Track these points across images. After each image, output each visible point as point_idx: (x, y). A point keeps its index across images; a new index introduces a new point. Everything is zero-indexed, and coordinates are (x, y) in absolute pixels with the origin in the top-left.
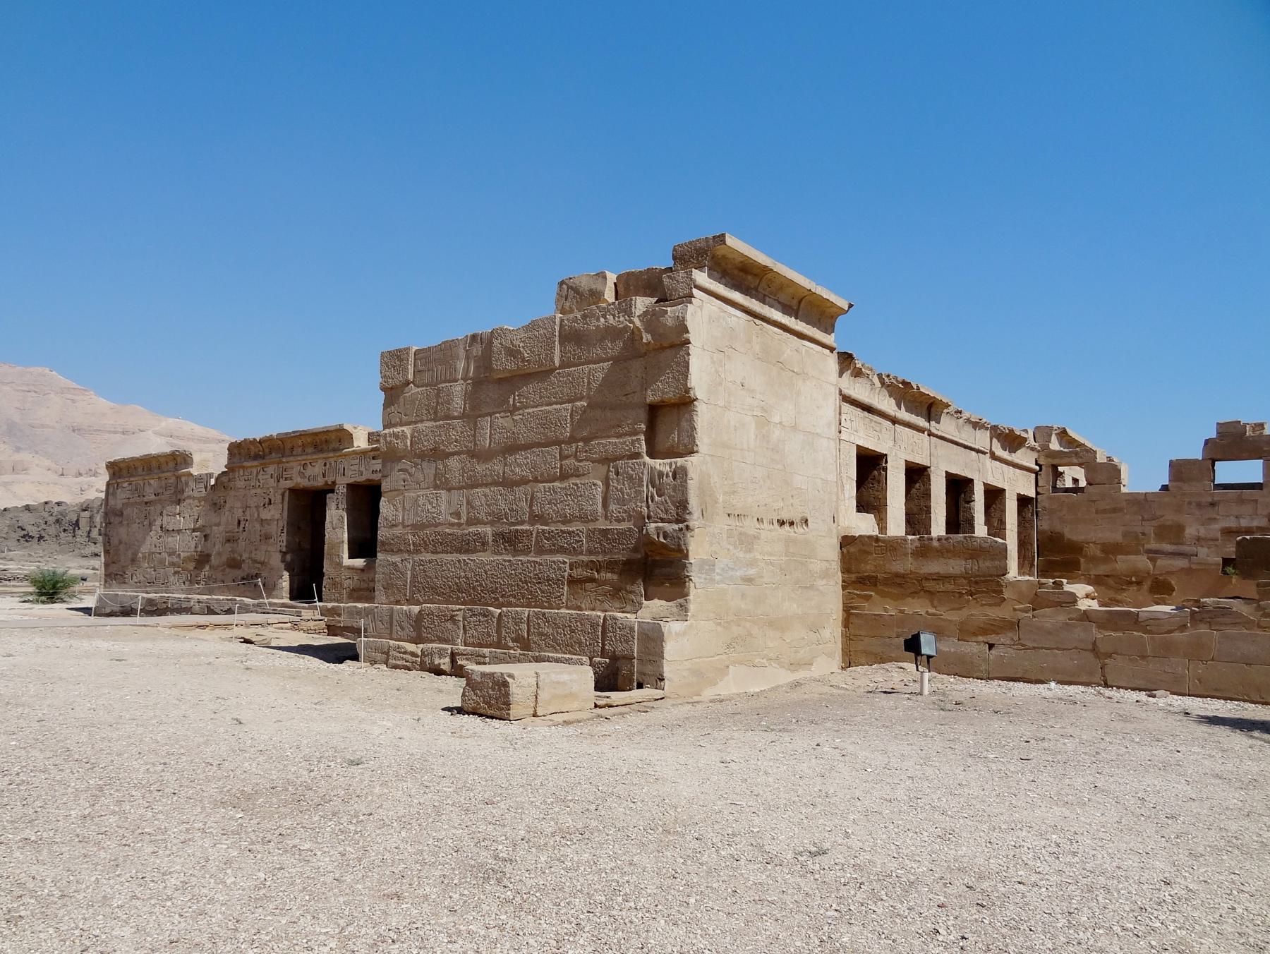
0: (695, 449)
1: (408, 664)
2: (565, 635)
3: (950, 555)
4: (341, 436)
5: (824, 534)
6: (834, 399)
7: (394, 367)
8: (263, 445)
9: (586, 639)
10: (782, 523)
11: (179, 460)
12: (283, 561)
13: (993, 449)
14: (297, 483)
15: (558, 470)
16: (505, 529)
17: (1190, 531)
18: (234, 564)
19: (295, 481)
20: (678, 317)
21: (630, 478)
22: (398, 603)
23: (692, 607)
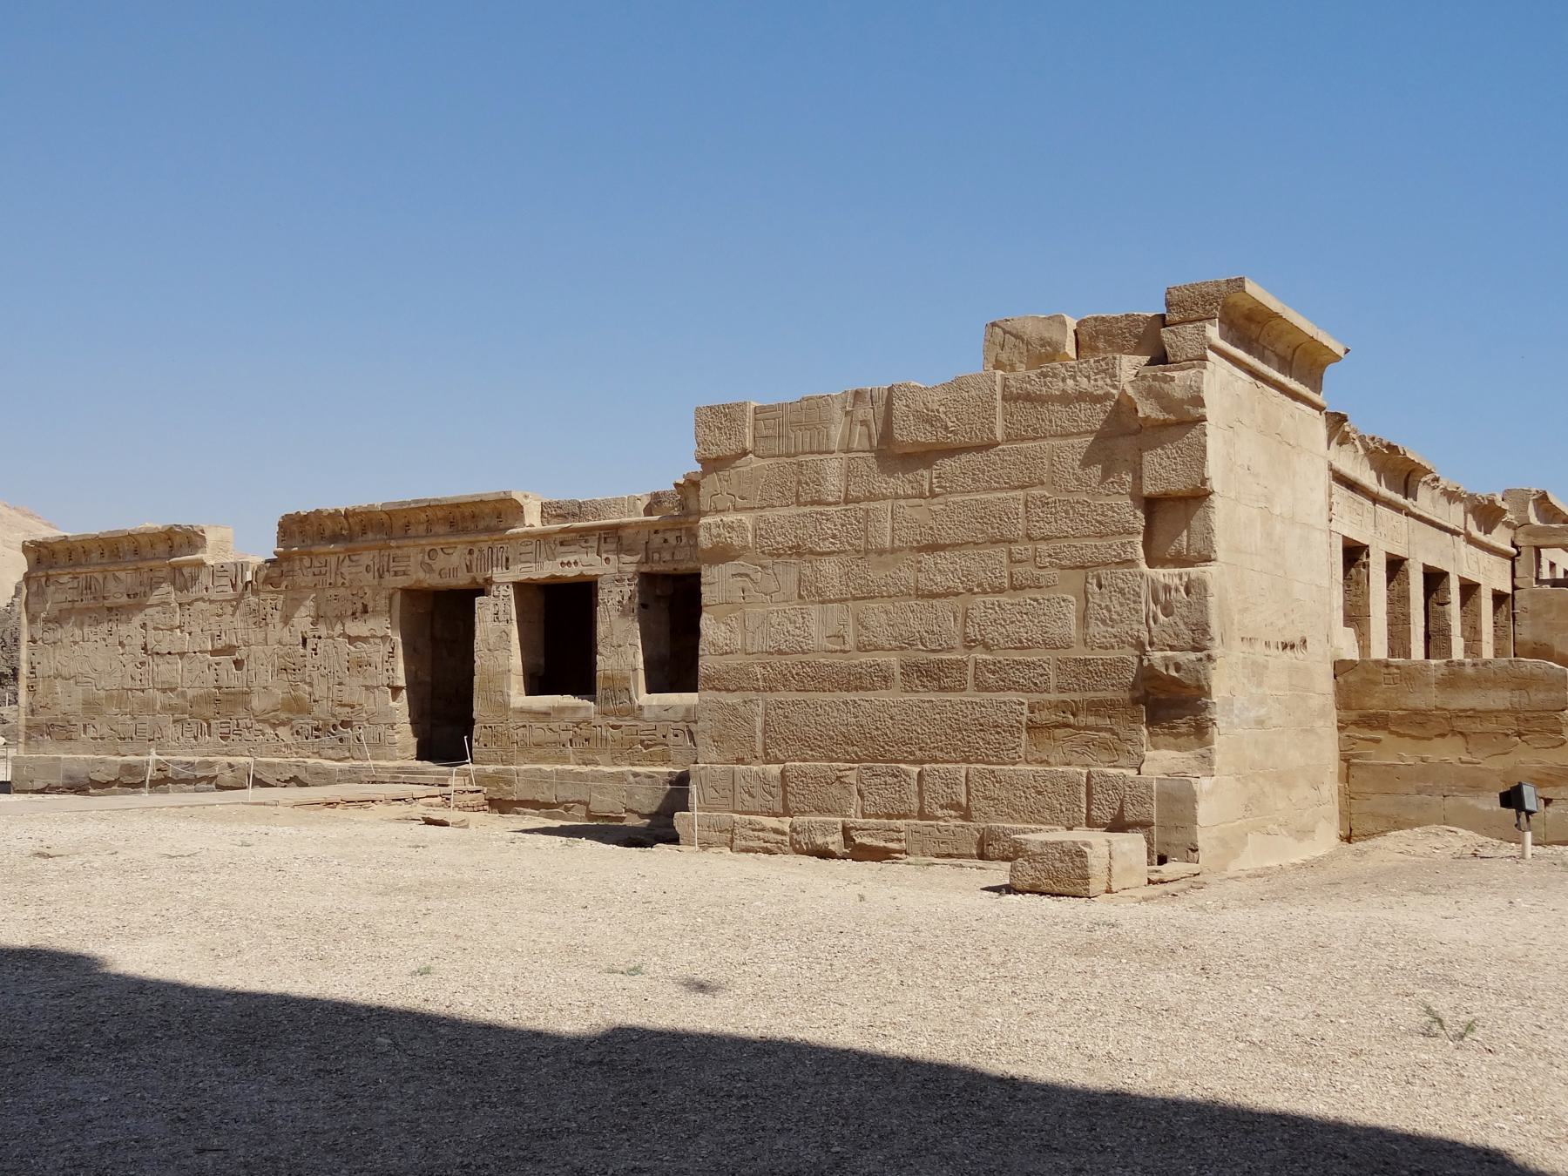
0: (1213, 557)
1: (768, 845)
2: (1027, 798)
3: (1489, 685)
4: (507, 510)
5: (1320, 660)
6: (1325, 477)
7: (720, 429)
8: (351, 520)
9: (1061, 804)
10: (1285, 646)
11: (181, 540)
13: (1468, 528)
14: (418, 581)
15: (1006, 580)
16: (922, 657)
19: (414, 577)
20: (1190, 386)
21: (1122, 592)
22: (740, 761)
23: (1217, 758)
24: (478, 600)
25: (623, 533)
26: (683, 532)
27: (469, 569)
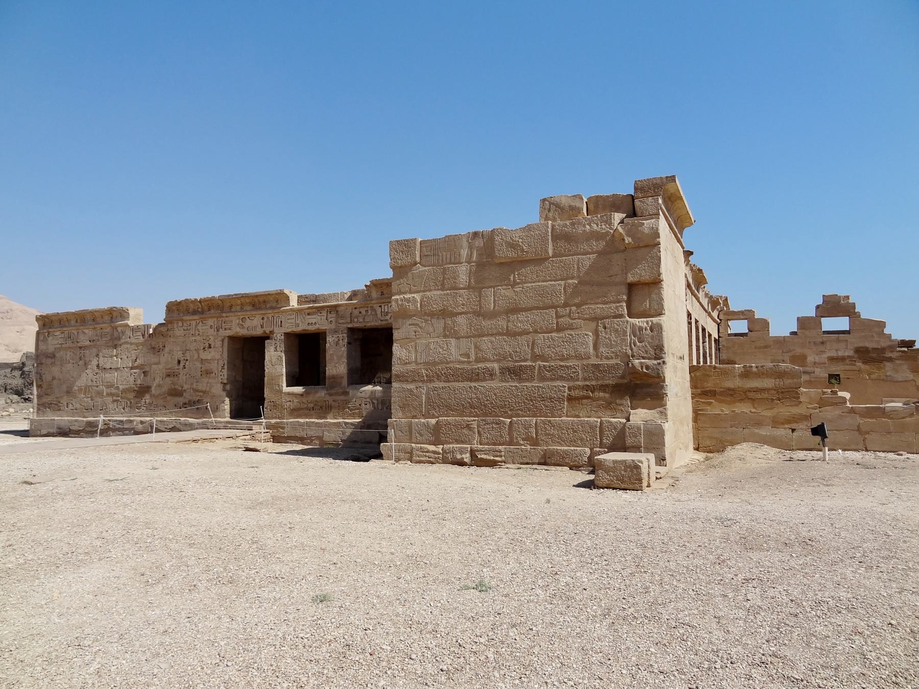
0: (663, 312)
1: (431, 459)
2: (568, 434)
3: (765, 376)
4: (280, 298)
7: (402, 252)
9: (586, 437)
11: (116, 315)
12: (224, 390)
14: (237, 333)
15: (555, 325)
16: (511, 364)
17: (810, 359)
18: (175, 393)
20: (653, 227)
21: (617, 330)
22: (414, 417)
23: (669, 413)
24: (266, 342)
25: (340, 309)
26: (369, 308)
27: (262, 326)
